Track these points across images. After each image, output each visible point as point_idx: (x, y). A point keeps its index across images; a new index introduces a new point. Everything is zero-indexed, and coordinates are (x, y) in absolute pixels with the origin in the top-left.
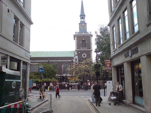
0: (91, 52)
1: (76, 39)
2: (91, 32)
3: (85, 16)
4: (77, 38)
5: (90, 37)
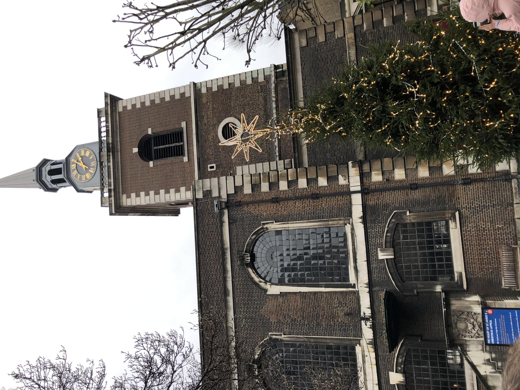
0: (204, 91)
1: (138, 195)
2: (99, 111)
3: (45, 162)
4: (133, 195)
5: (120, 109)
